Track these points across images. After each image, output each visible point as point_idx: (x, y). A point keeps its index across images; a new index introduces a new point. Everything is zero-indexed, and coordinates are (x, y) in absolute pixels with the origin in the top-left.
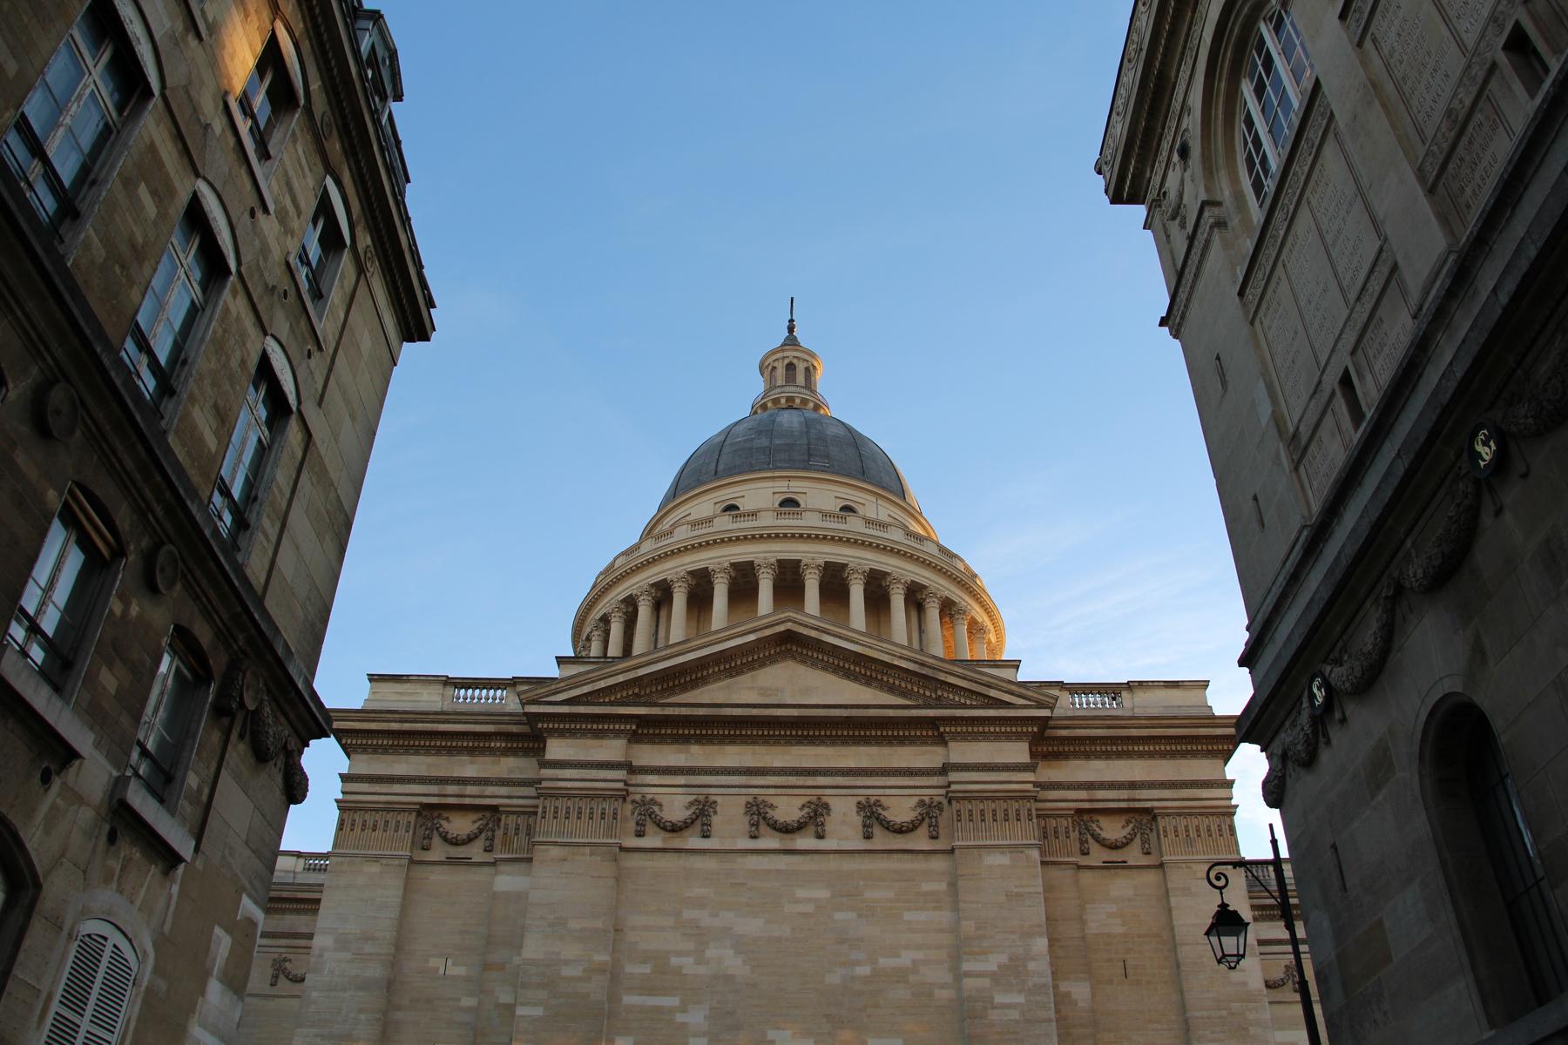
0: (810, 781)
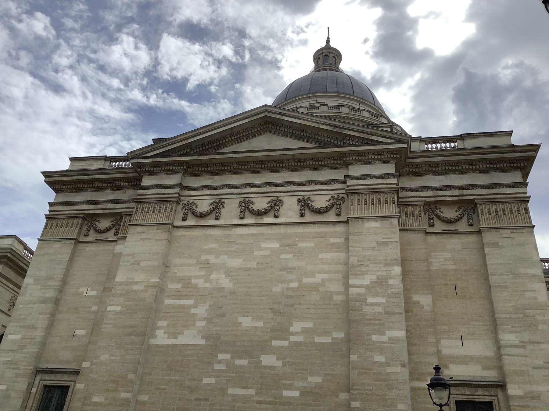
0: (273, 189)
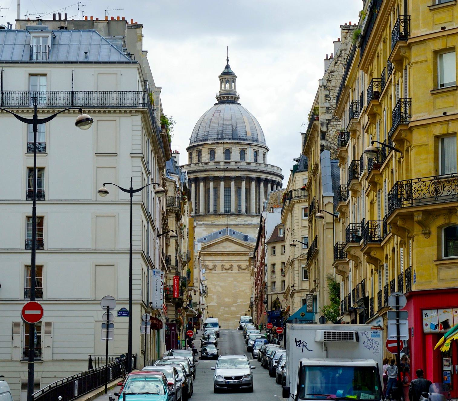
0: (230, 262)
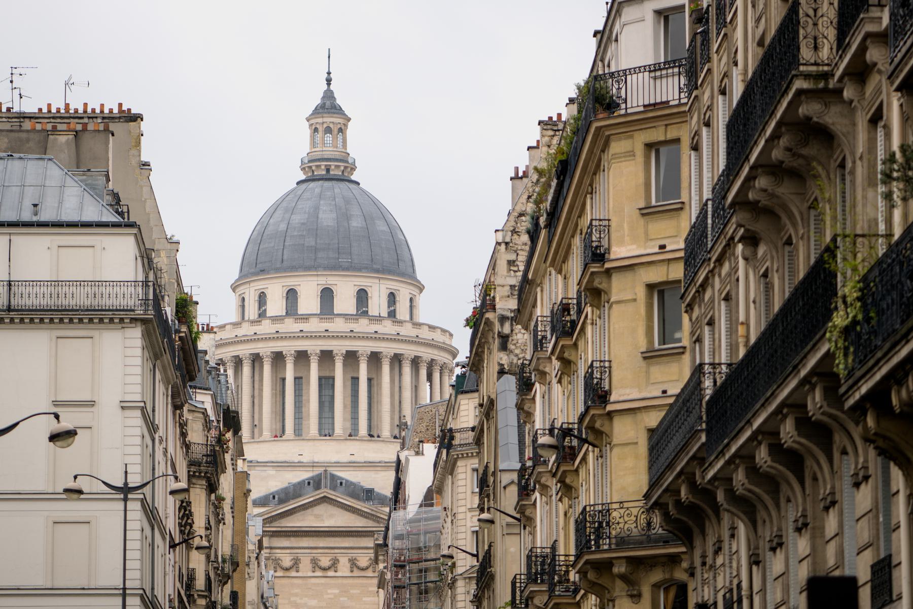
0: (332, 551)
